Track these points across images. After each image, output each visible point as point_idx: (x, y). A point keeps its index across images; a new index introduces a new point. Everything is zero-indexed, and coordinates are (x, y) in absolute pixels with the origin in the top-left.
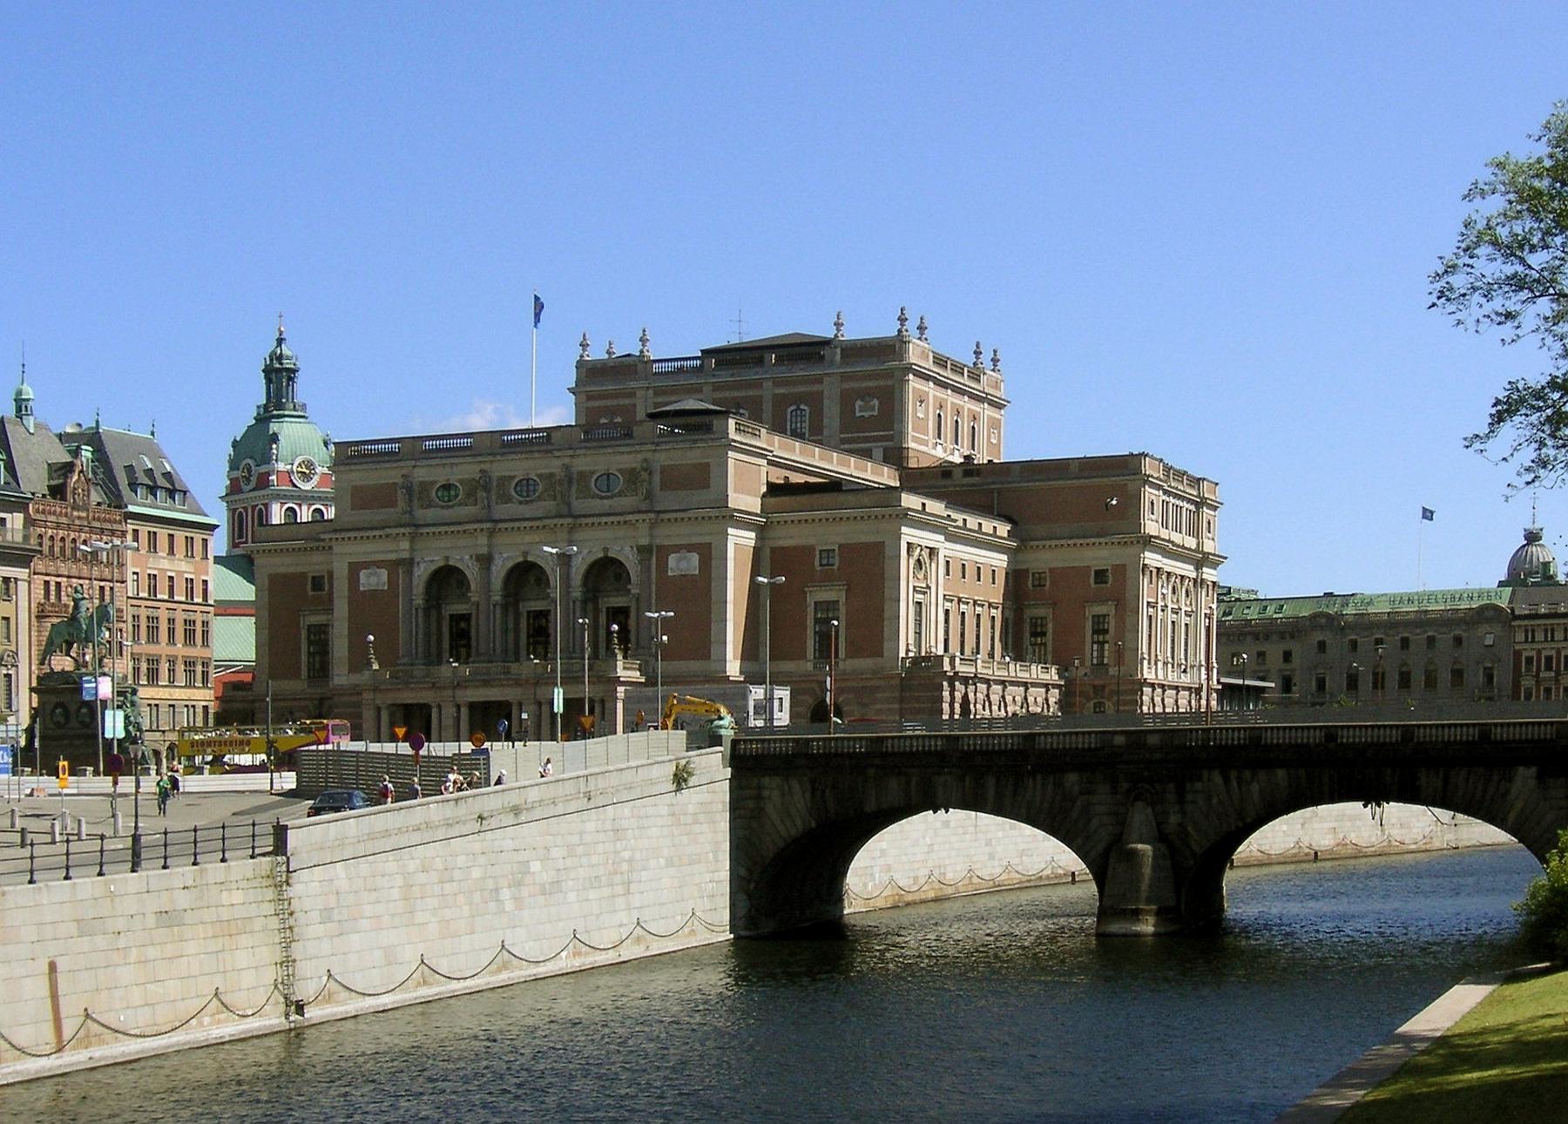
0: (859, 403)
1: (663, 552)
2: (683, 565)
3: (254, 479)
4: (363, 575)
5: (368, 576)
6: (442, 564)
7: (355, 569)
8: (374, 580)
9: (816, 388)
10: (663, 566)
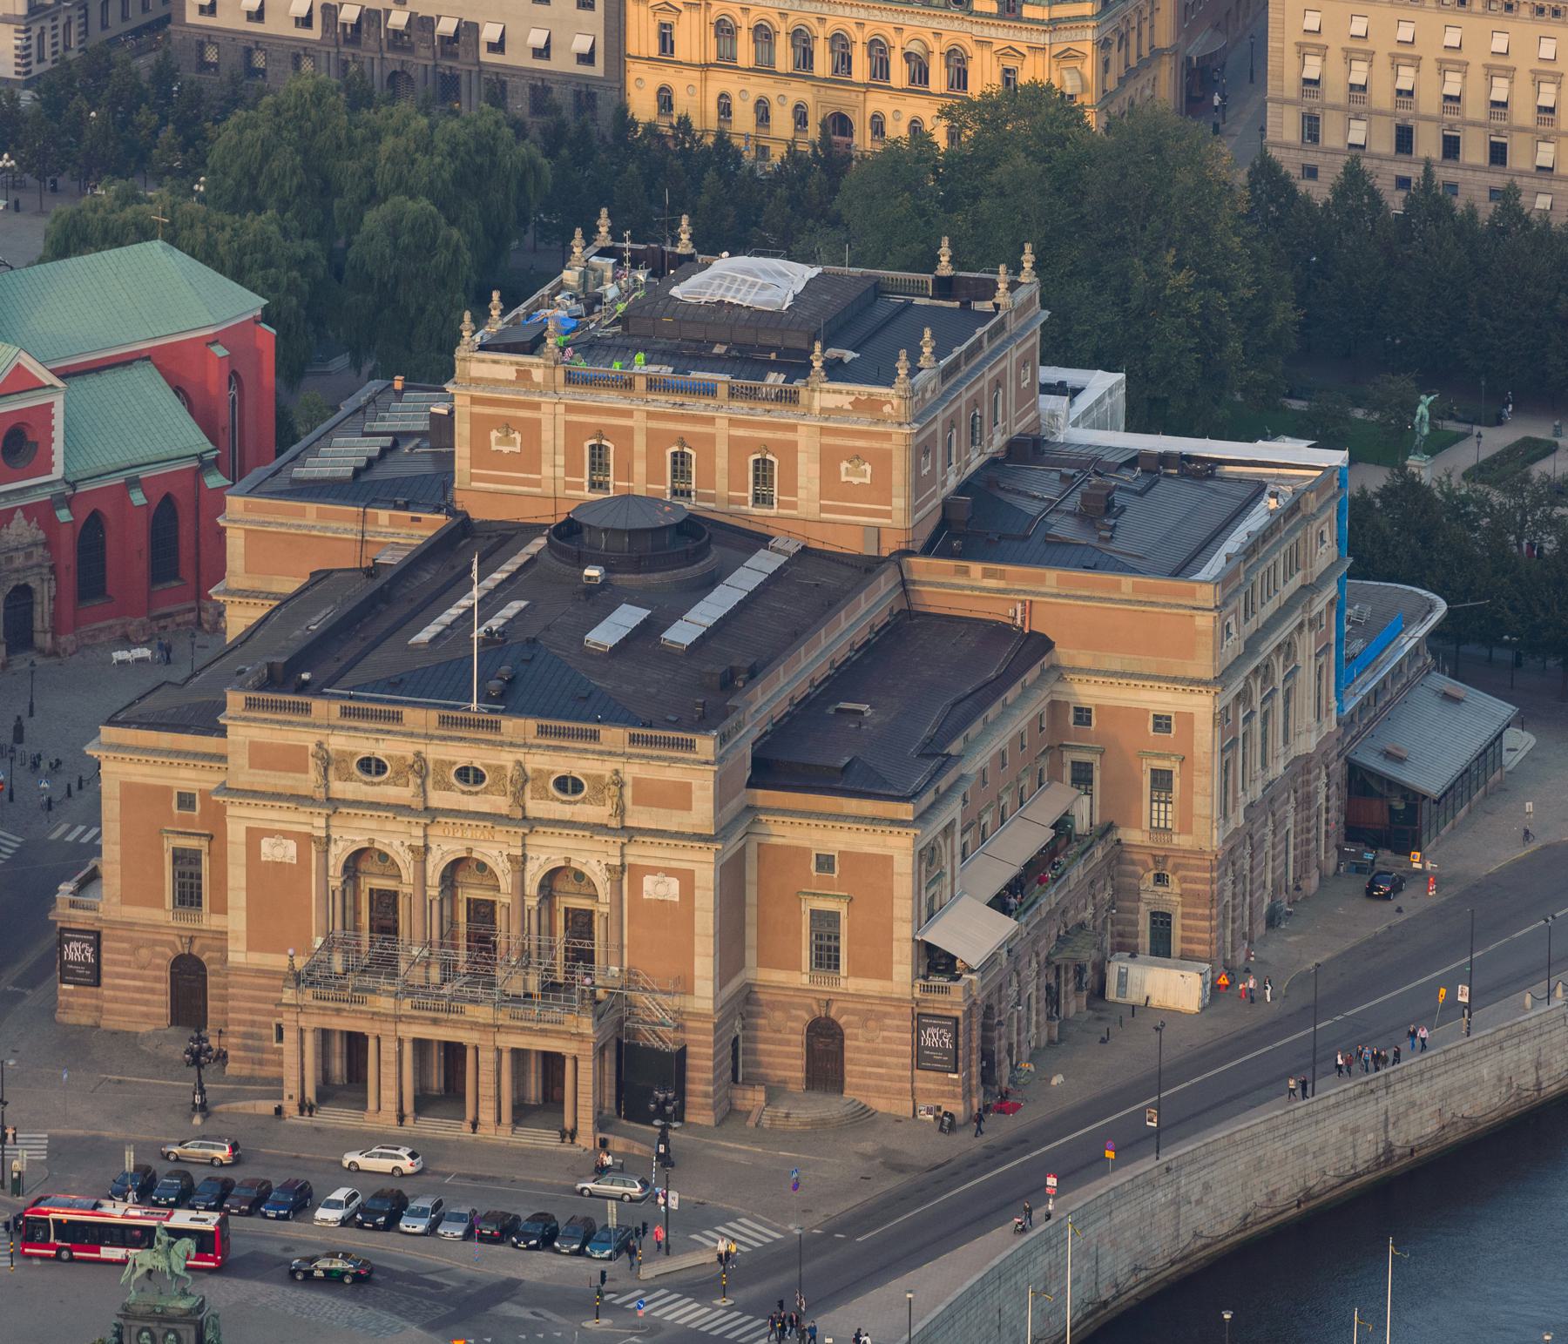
0: (844, 465)
1: (638, 872)
4: (266, 844)
7: (254, 837)
9: (789, 436)
10: (637, 888)
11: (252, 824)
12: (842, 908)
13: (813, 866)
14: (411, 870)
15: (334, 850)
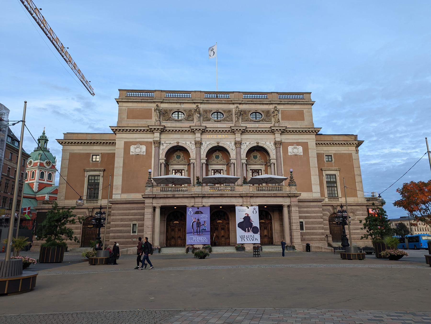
2: (295, 150)
3: (32, 165)
4: (132, 148)
6: (176, 144)
7: (127, 145)
8: (138, 150)
10: (286, 151)
11: (126, 140)
12: (337, 173)
14: (194, 153)
15: (162, 147)
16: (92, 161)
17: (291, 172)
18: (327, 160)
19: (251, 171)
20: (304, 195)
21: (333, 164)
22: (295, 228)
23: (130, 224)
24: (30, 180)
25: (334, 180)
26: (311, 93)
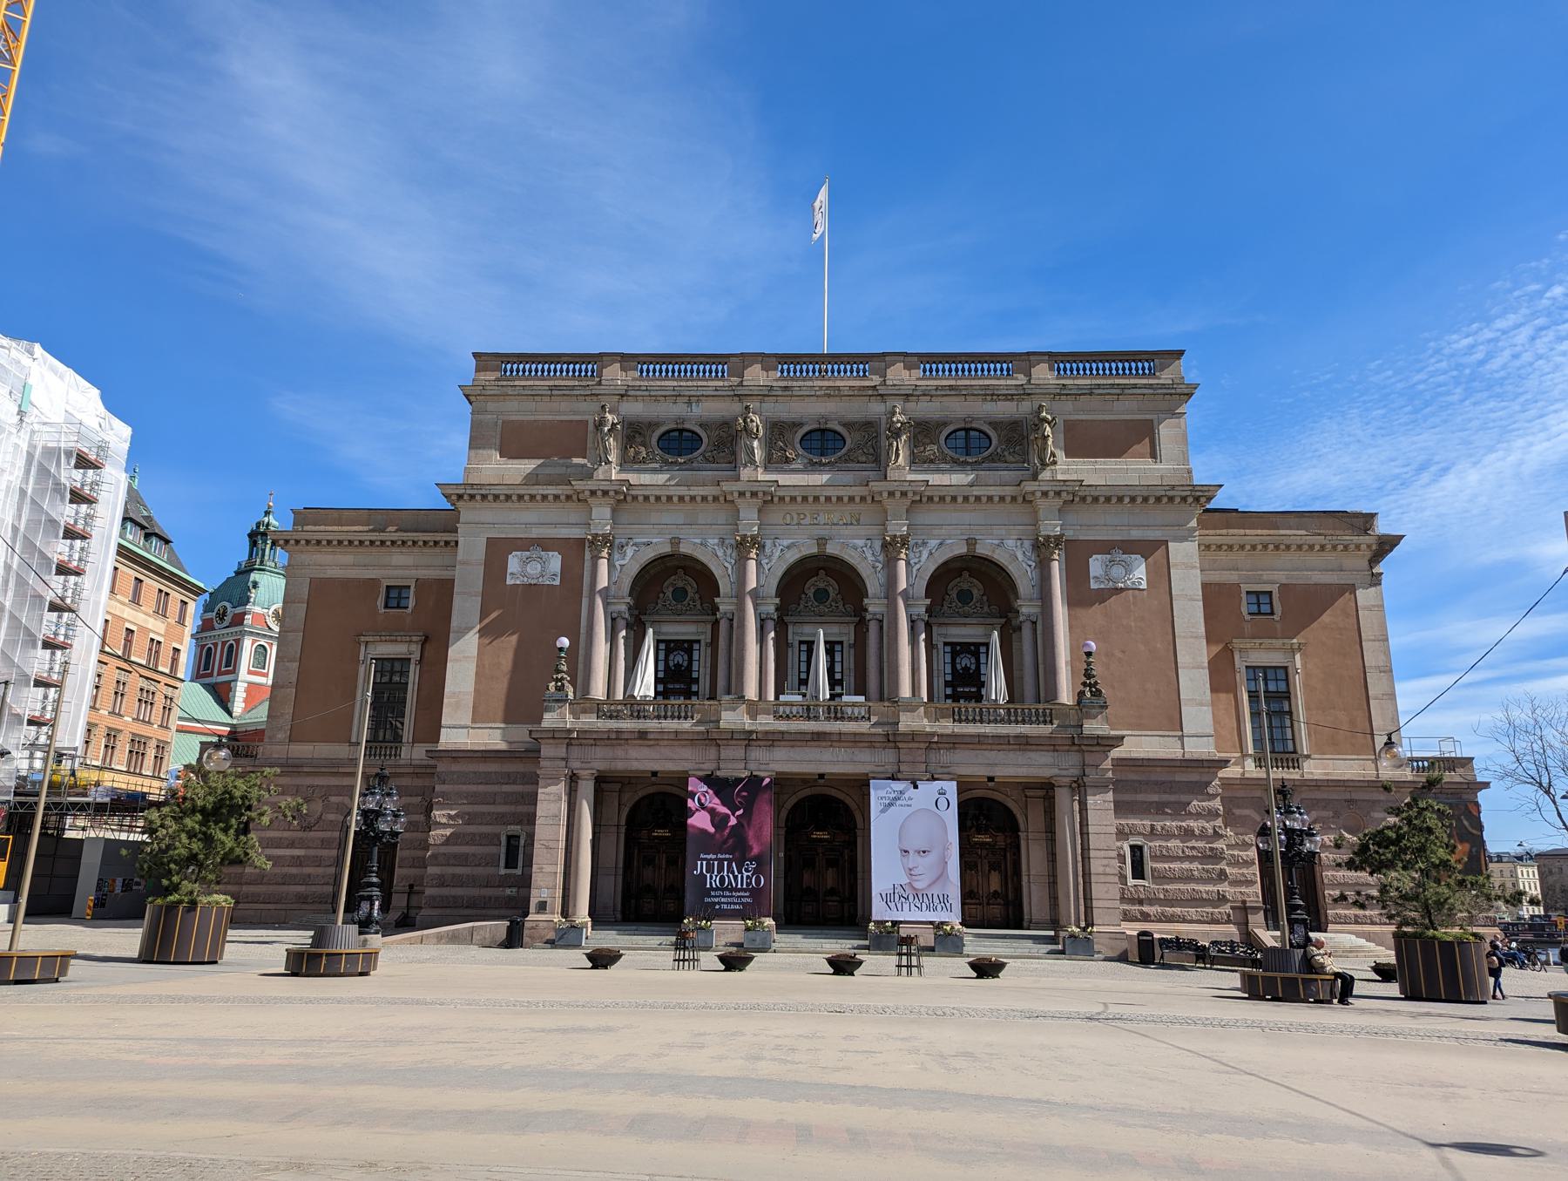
3: (228, 619)
4: (514, 563)
5: (525, 562)
6: (667, 549)
7: (498, 550)
8: (534, 569)
13: (1244, 610)
16: (386, 607)
17: (1089, 654)
18: (1254, 608)
19: (948, 649)
20: (1141, 745)
21: (1278, 626)
22: (1101, 870)
23: (498, 836)
24: (219, 674)
25: (1282, 686)
26: (1181, 353)
